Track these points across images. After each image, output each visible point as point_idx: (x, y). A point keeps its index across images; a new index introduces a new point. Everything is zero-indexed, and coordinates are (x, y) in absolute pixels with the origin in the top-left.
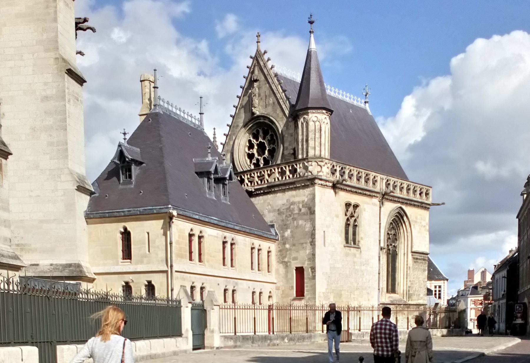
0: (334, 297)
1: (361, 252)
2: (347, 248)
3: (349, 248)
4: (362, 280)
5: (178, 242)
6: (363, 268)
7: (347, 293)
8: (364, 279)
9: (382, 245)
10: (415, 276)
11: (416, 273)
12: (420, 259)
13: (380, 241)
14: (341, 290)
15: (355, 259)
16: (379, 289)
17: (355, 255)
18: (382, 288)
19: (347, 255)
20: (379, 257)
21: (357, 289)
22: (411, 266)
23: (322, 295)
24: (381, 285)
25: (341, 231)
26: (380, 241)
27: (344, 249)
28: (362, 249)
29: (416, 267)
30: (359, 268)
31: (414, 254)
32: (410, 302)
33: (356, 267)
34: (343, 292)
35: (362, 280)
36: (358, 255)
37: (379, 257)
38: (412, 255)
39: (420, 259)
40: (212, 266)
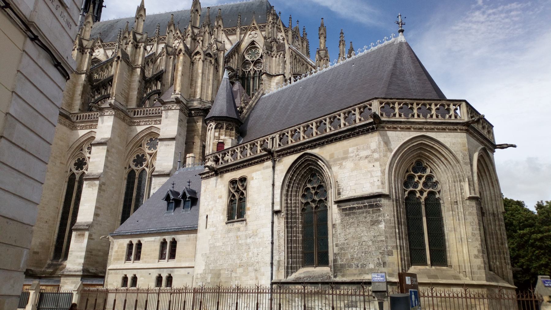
0: (211, 278)
1: (246, 223)
2: (229, 224)
3: (232, 224)
4: (248, 255)
5: (117, 252)
6: (249, 241)
7: (226, 272)
8: (250, 254)
9: (277, 208)
10: (350, 236)
11: (352, 230)
12: (359, 208)
13: (273, 203)
14: (220, 270)
15: (239, 233)
16: (272, 264)
17: (239, 229)
18: (279, 262)
19: (229, 231)
20: (273, 223)
21: (240, 266)
22: (338, 222)
23: (199, 276)
24: (276, 258)
25: (224, 210)
26: (273, 203)
27: (226, 226)
28: (247, 220)
29: (351, 220)
30: (243, 242)
31: (340, 204)
32: (338, 279)
33: (240, 242)
34: (222, 272)
35: (248, 255)
36: (242, 229)
37: (273, 223)
38: (338, 206)
39: (359, 208)
40: (146, 262)
